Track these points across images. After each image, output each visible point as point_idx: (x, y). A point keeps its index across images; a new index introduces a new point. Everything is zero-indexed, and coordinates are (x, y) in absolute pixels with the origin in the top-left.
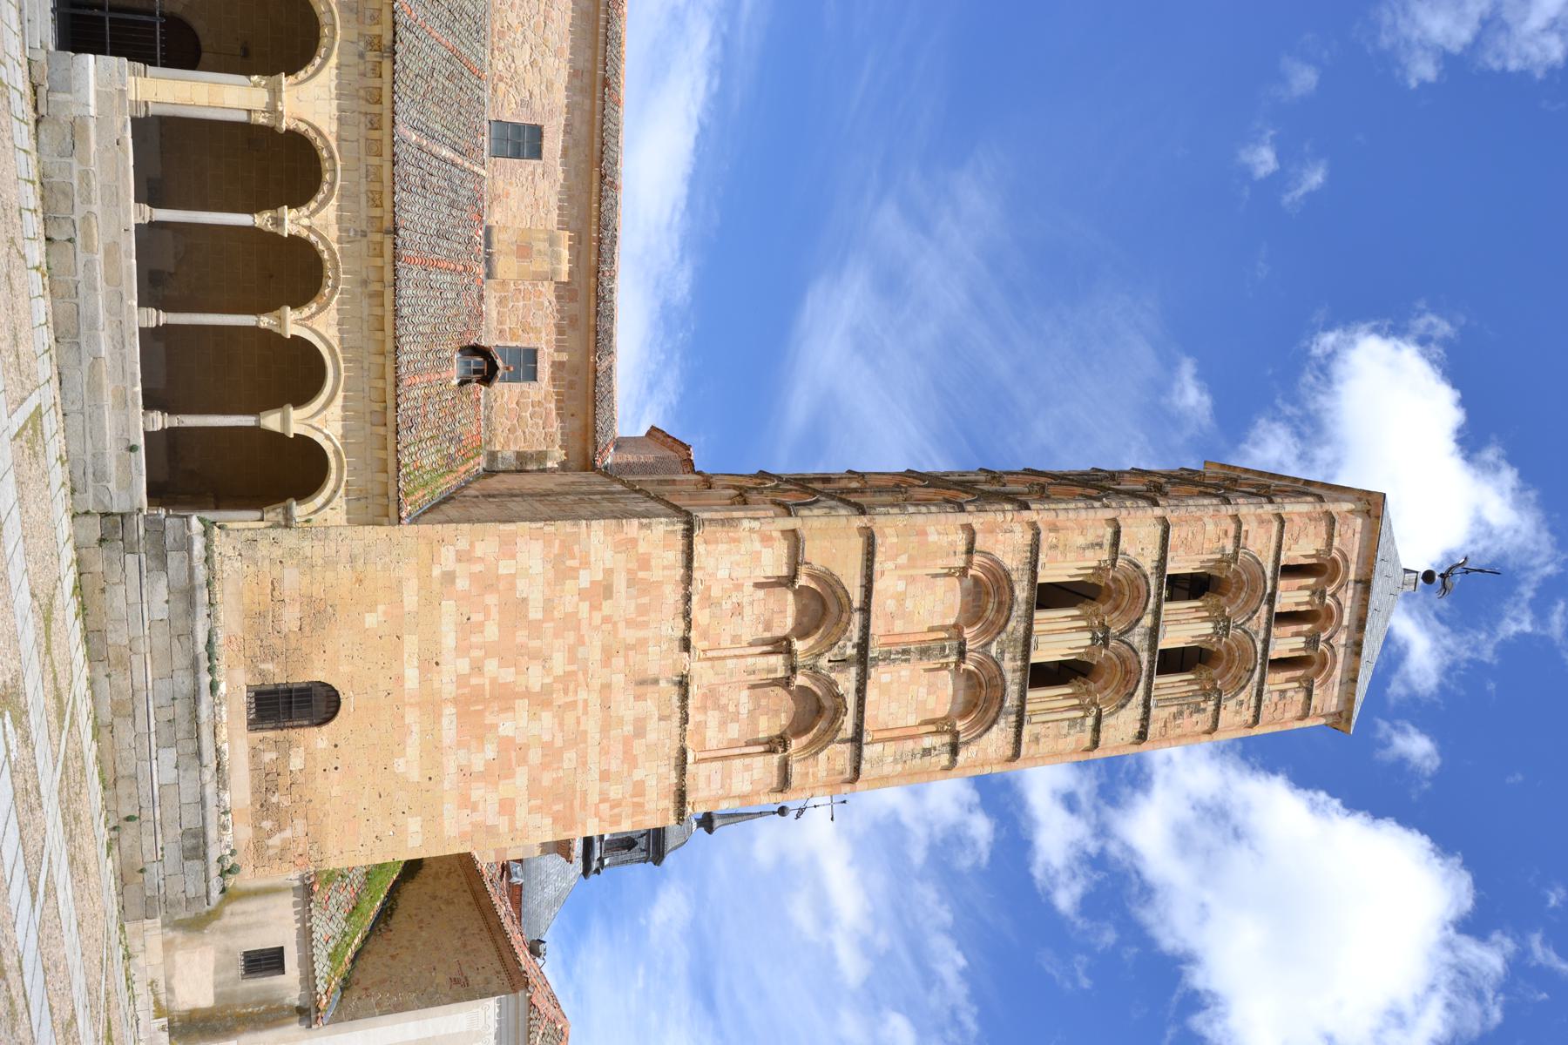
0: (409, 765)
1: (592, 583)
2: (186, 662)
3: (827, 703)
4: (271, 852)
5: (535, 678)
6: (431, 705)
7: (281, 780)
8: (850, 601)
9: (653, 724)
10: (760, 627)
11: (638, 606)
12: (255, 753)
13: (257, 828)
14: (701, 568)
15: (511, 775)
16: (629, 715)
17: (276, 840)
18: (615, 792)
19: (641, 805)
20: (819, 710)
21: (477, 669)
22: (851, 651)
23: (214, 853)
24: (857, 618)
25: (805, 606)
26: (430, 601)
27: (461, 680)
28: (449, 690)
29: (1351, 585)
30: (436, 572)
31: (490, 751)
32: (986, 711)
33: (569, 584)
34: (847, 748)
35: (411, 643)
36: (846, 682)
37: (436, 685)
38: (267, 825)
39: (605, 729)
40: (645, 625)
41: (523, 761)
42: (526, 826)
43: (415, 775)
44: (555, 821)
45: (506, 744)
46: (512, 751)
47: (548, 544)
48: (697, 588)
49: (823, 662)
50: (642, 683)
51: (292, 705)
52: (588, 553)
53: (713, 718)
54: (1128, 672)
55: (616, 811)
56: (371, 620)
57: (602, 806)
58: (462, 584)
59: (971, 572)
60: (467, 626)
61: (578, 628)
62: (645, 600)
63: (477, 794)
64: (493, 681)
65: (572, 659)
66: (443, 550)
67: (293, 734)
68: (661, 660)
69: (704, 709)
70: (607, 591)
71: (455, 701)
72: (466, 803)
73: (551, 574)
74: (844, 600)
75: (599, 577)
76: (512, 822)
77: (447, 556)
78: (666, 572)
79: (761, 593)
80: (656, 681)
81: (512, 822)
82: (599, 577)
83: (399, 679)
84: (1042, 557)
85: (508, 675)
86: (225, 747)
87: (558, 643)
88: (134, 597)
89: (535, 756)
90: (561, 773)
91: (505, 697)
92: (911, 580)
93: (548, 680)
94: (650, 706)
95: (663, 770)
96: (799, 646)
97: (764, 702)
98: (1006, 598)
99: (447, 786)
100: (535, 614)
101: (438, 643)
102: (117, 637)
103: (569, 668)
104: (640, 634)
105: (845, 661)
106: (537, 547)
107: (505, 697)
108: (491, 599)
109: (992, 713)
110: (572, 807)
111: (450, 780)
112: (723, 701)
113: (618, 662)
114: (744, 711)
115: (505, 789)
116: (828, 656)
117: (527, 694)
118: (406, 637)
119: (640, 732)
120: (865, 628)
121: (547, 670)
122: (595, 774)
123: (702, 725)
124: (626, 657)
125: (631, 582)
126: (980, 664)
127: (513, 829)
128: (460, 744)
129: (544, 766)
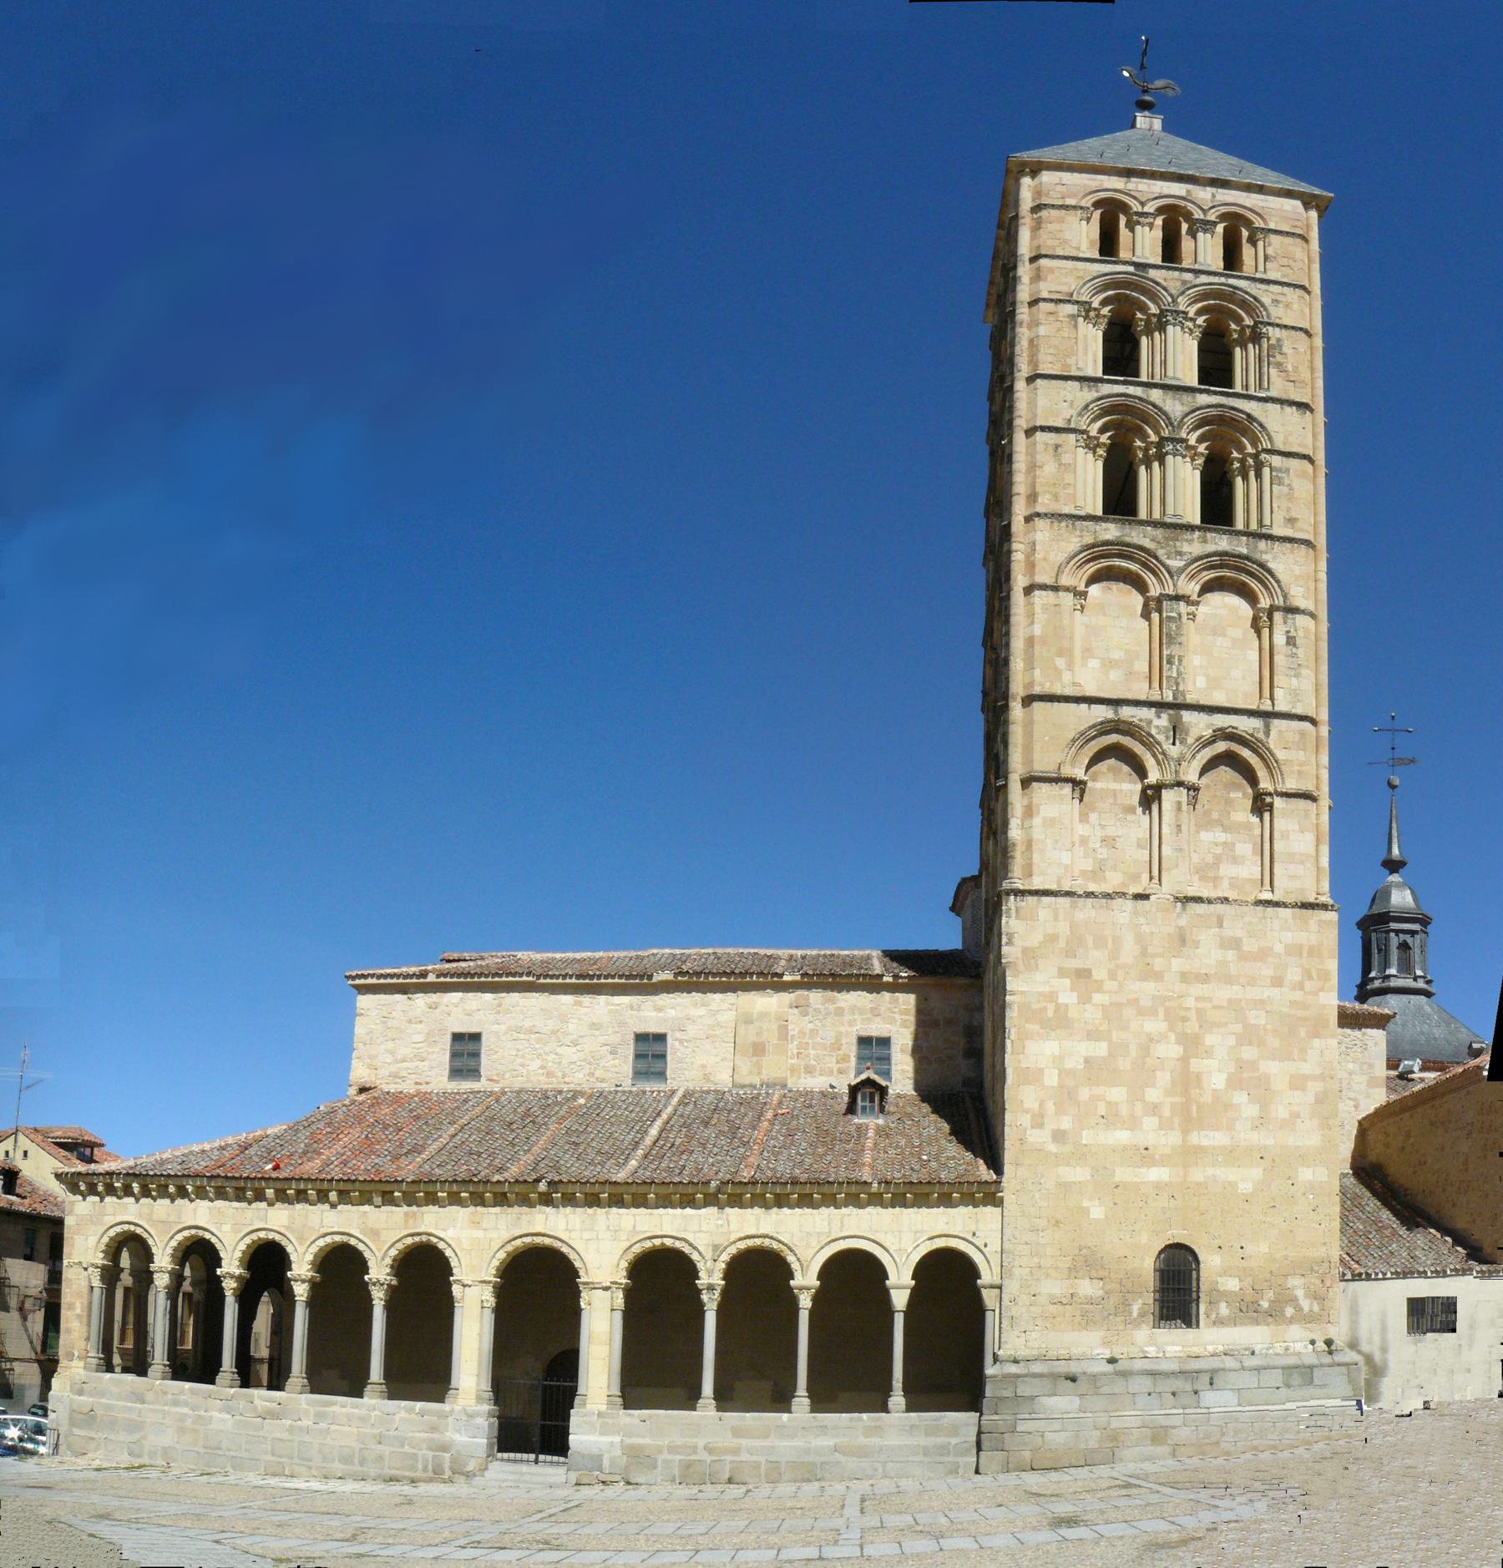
0: (1246, 1178)
2: (1121, 1382)
4: (1316, 1308)
5: (1170, 1050)
6: (1189, 1155)
7: (1248, 1299)
10: (1130, 817)
12: (1220, 1322)
13: (1291, 1321)
16: (1217, 955)
17: (1305, 1304)
18: (1293, 974)
19: (1311, 948)
21: (1154, 1109)
22: (1164, 721)
23: (1310, 1360)
24: (1126, 712)
25: (1110, 769)
26: (1081, 1155)
27: (1164, 1126)
30: (1053, 1148)
31: (1240, 1098)
35: (1123, 1174)
37: (1168, 1151)
38: (1289, 1311)
39: (1228, 980)
41: (1253, 1065)
43: (1257, 1173)
44: (1317, 1035)
45: (1234, 1082)
46: (1244, 1077)
48: (1079, 886)
49: (1174, 751)
51: (1177, 1288)
52: (1040, 994)
53: (1227, 870)
55: (1314, 974)
56: (1097, 1212)
57: (1307, 988)
58: (1066, 1123)
59: (1082, 587)
60: (1111, 1118)
61: (1119, 1005)
64: (1168, 1093)
65: (1153, 1012)
66: (1030, 1139)
67: (1204, 1287)
68: (1159, 920)
69: (1216, 880)
70: (1083, 974)
71: (1185, 1132)
75: (1067, 982)
76: (1314, 1078)
77: (1036, 1137)
79: (1093, 817)
81: (1314, 1078)
82: (1067, 982)
83: (1158, 1186)
84: (1066, 510)
85: (1164, 1078)
86: (1210, 1348)
88: (1056, 1425)
89: (1249, 1053)
91: (1187, 1082)
92: (1088, 652)
93: (1172, 1037)
96: (1153, 777)
97: (1215, 816)
99: (1270, 1142)
100: (1101, 1049)
101: (1125, 1148)
102: (1092, 1439)
105: (1176, 729)
106: (1031, 1047)
107: (1187, 1082)
108: (1084, 1094)
111: (1265, 1138)
112: (1210, 859)
113: (1158, 964)
114: (1222, 837)
116: (1167, 746)
117: (1185, 1059)
118: (1117, 1179)
119: (1235, 944)
120: (1137, 703)
121: (1163, 1038)
122: (1275, 992)
123: (1235, 883)
124: (1155, 955)
127: (1322, 1077)
128: (1230, 1127)
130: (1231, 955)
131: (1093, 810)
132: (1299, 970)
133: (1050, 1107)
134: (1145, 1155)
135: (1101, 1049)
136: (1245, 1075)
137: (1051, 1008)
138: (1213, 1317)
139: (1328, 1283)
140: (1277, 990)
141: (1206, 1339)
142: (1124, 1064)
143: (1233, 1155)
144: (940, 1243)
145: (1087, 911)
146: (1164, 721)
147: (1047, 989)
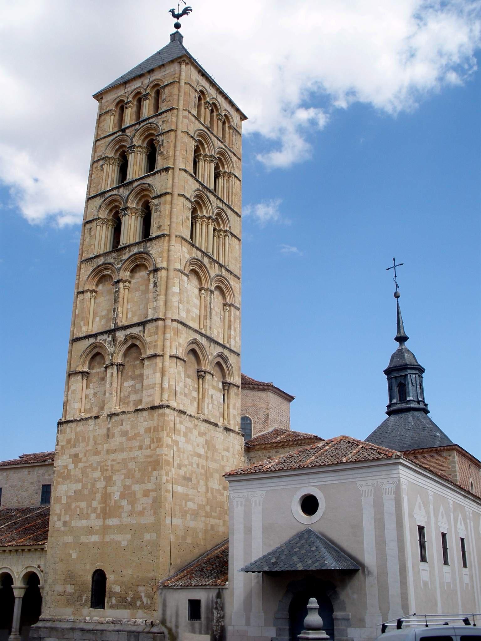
0: (124, 539)
3: (129, 343)
4: (149, 602)
5: (101, 484)
7: (123, 596)
8: (92, 344)
9: (123, 428)
10: (103, 382)
11: (82, 442)
12: (112, 607)
13: (139, 608)
14: (73, 416)
15: (134, 493)
17: (145, 600)
18: (147, 442)
19: (154, 427)
20: (133, 346)
21: (94, 510)
24: (99, 338)
28: (100, 522)
29: (126, 91)
30: (63, 529)
31: (124, 503)
32: (145, 259)
33: (72, 473)
34: (148, 326)
35: (83, 539)
37: (98, 528)
38: (138, 603)
39: (122, 450)
40: (89, 437)
41: (129, 487)
42: (155, 484)
43: (128, 536)
44: (155, 470)
46: (127, 494)
47: (58, 483)
50: (108, 436)
54: (143, 190)
55: (155, 440)
56: (74, 556)
58: (67, 518)
60: (82, 516)
62: (81, 438)
63: (139, 508)
64: (100, 503)
65: (96, 469)
67: (107, 590)
69: (128, 403)
70: (76, 456)
71: (104, 519)
72: (141, 513)
73: (68, 481)
75: (71, 460)
79: (91, 385)
80: (108, 429)
82: (71, 460)
83: (94, 543)
85: (98, 496)
86: (107, 619)
87: (90, 476)
89: (128, 482)
90: (137, 469)
93: (102, 478)
94: (116, 431)
95: (142, 419)
97: (130, 374)
99: (134, 522)
100: (79, 486)
103: (99, 470)
105: (114, 339)
107: (106, 496)
108: (73, 505)
109: (145, 256)
110: (151, 462)
111: (132, 521)
112: (127, 394)
115: (139, 495)
117: (106, 488)
118: (81, 541)
119: (125, 434)
120: (102, 333)
122: (139, 453)
125: (75, 446)
126: (126, 270)
127: (155, 490)
128: (120, 517)
129: (133, 477)
130: (124, 439)
132: (149, 439)
133: (63, 512)
134: (90, 531)
135: (79, 486)
136: (127, 492)
138: (110, 604)
139: (154, 590)
141: (108, 614)
142: (86, 492)
143: (121, 529)
144: (29, 570)
145: (81, 427)
146: (110, 339)
147: (65, 464)
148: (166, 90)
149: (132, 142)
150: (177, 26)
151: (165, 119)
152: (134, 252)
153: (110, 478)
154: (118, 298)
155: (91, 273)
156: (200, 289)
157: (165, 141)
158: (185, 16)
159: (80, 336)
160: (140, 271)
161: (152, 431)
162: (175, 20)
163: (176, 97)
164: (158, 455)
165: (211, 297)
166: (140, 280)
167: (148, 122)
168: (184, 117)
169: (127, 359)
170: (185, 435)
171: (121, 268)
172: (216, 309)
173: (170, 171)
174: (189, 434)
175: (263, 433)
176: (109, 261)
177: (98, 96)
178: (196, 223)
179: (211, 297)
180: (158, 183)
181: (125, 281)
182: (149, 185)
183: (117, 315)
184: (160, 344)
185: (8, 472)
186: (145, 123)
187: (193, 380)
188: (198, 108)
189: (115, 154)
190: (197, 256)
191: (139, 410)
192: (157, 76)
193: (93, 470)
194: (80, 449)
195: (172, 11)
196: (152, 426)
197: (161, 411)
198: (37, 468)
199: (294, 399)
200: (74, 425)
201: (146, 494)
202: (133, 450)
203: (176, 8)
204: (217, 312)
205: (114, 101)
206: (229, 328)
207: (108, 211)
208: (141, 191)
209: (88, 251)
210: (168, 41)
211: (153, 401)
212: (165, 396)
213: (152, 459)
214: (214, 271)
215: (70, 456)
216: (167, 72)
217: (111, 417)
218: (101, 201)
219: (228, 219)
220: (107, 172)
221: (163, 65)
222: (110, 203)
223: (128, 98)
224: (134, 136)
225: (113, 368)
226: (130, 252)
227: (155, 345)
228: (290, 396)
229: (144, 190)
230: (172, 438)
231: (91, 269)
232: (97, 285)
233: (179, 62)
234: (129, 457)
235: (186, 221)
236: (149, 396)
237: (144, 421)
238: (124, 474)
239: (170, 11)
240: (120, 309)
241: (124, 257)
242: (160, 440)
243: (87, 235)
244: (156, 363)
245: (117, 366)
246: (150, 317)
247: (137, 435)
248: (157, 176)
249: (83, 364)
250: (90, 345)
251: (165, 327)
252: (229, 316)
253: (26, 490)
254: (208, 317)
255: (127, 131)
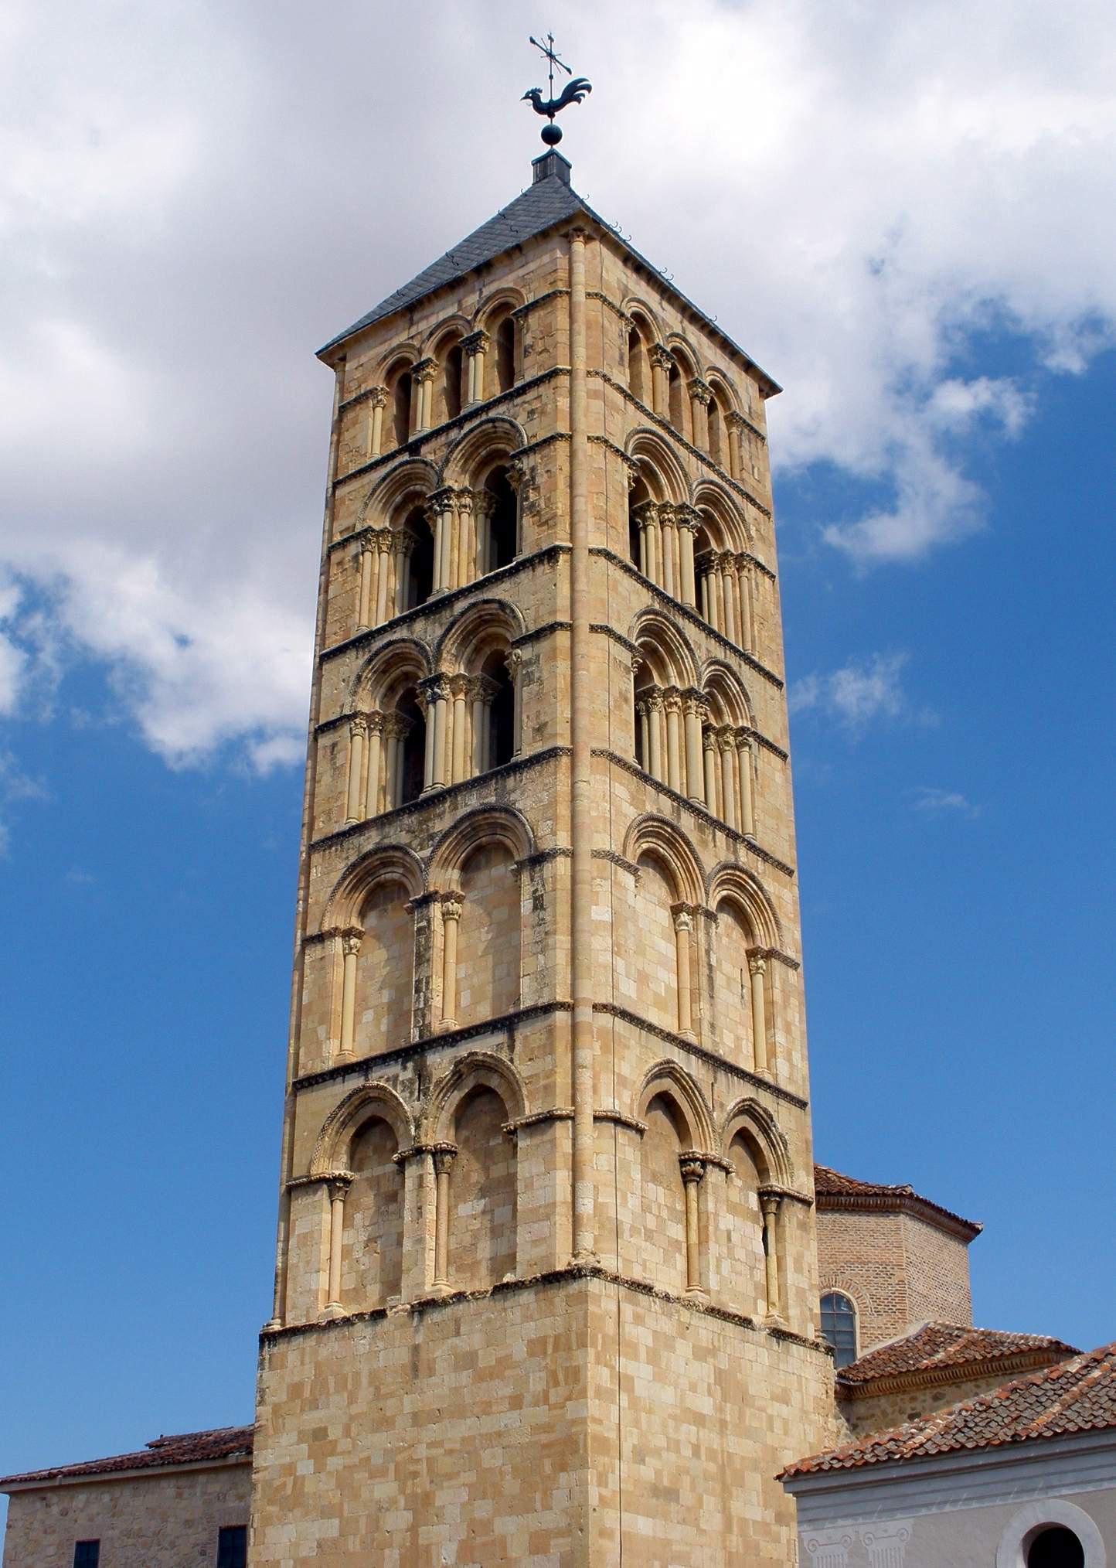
1: (309, 1457)
5: (399, 1520)
10: (392, 1207)
11: (337, 1392)
14: (307, 1315)
18: (537, 1383)
19: (557, 1338)
20: (481, 1092)
29: (413, 331)
32: (504, 827)
33: (309, 1487)
34: (523, 1032)
36: (441, 1063)
39: (459, 1412)
41: (487, 1525)
42: (565, 1511)
44: (563, 1467)
47: (267, 1521)
54: (483, 622)
55: (561, 1377)
57: (552, 1400)
62: (331, 1381)
65: (382, 1473)
70: (320, 1434)
73: (298, 1512)
74: (356, 1101)
75: (305, 1446)
78: (307, 1360)
79: (358, 1216)
80: (416, 1349)
82: (305, 1446)
87: (365, 1494)
89: (483, 1509)
90: (508, 1468)
93: (402, 1503)
94: (441, 1353)
98: (374, 860)
100: (331, 1528)
104: (364, 1381)
105: (422, 1075)
109: (502, 818)
112: (467, 1239)
117: (413, 1529)
119: (466, 1361)
120: (384, 1059)
122: (511, 1418)
125: (314, 1405)
126: (446, 863)
127: (567, 1532)
130: (465, 1377)
131: (357, 1209)
132: (543, 1374)
135: (331, 1528)
137: (290, 1481)
140: (516, 1414)
142: (353, 1544)
145: (331, 1346)
146: (408, 1074)
147: (288, 1459)
148: (533, 320)
149: (441, 480)
150: (551, 136)
151: (536, 405)
152: (469, 809)
153: (427, 1498)
154: (428, 948)
155: (344, 878)
156: (676, 911)
157: (540, 470)
158: (572, 105)
159: (319, 1071)
160: (489, 864)
161: (550, 1351)
162: (544, 121)
163: (563, 338)
164: (574, 1422)
165: (708, 933)
166: (489, 891)
167: (484, 417)
168: (594, 394)
169: (465, 1133)
170: (653, 1358)
171: (430, 858)
172: (727, 967)
173: (563, 558)
174: (664, 1354)
175: (889, 1342)
176: (393, 841)
177: (334, 355)
178: (648, 712)
179: (708, 933)
180: (526, 598)
181: (447, 898)
182: (502, 604)
183: (426, 1001)
184: (562, 1080)
185: (117, 1491)
186: (476, 422)
187: (668, 1188)
188: (630, 366)
189: (393, 521)
190: (659, 810)
191: (507, 1286)
192: (505, 280)
193: (371, 1477)
194: (331, 1414)
195: (534, 96)
196: (550, 1332)
197: (575, 1287)
198: (202, 1479)
199: (978, 1232)
200: (309, 1342)
201: (538, 1544)
202: (494, 1408)
203: (542, 84)
204: (728, 978)
205: (379, 364)
206: (770, 1023)
207: (383, 690)
208: (480, 625)
209: (329, 813)
210: (525, 180)
211: (550, 1256)
212: (587, 1240)
213: (552, 1437)
214: (714, 853)
215: (302, 1437)
216: (532, 266)
217: (421, 1313)
218: (361, 661)
219: (746, 695)
220: (372, 574)
221: (518, 248)
222: (388, 666)
223: (420, 352)
224: (447, 461)
225: (422, 1162)
226: (456, 808)
227: (546, 1087)
228: (965, 1224)
229: (486, 622)
230: (612, 1368)
231: (341, 867)
232: (362, 915)
233: (566, 236)
234: (484, 1431)
235: (618, 707)
236: (535, 1243)
237: (526, 1320)
238: (470, 1486)
239: (526, 97)
240: (436, 983)
241: (440, 826)
242: (575, 1375)
243: (323, 766)
244: (553, 1142)
245: (434, 1155)
246: (526, 1003)
247: (505, 1362)
248: (524, 577)
249: (333, 1156)
250: (350, 1097)
251: (574, 1027)
252: (768, 988)
253: (173, 1545)
254: (705, 994)
255: (424, 449)
